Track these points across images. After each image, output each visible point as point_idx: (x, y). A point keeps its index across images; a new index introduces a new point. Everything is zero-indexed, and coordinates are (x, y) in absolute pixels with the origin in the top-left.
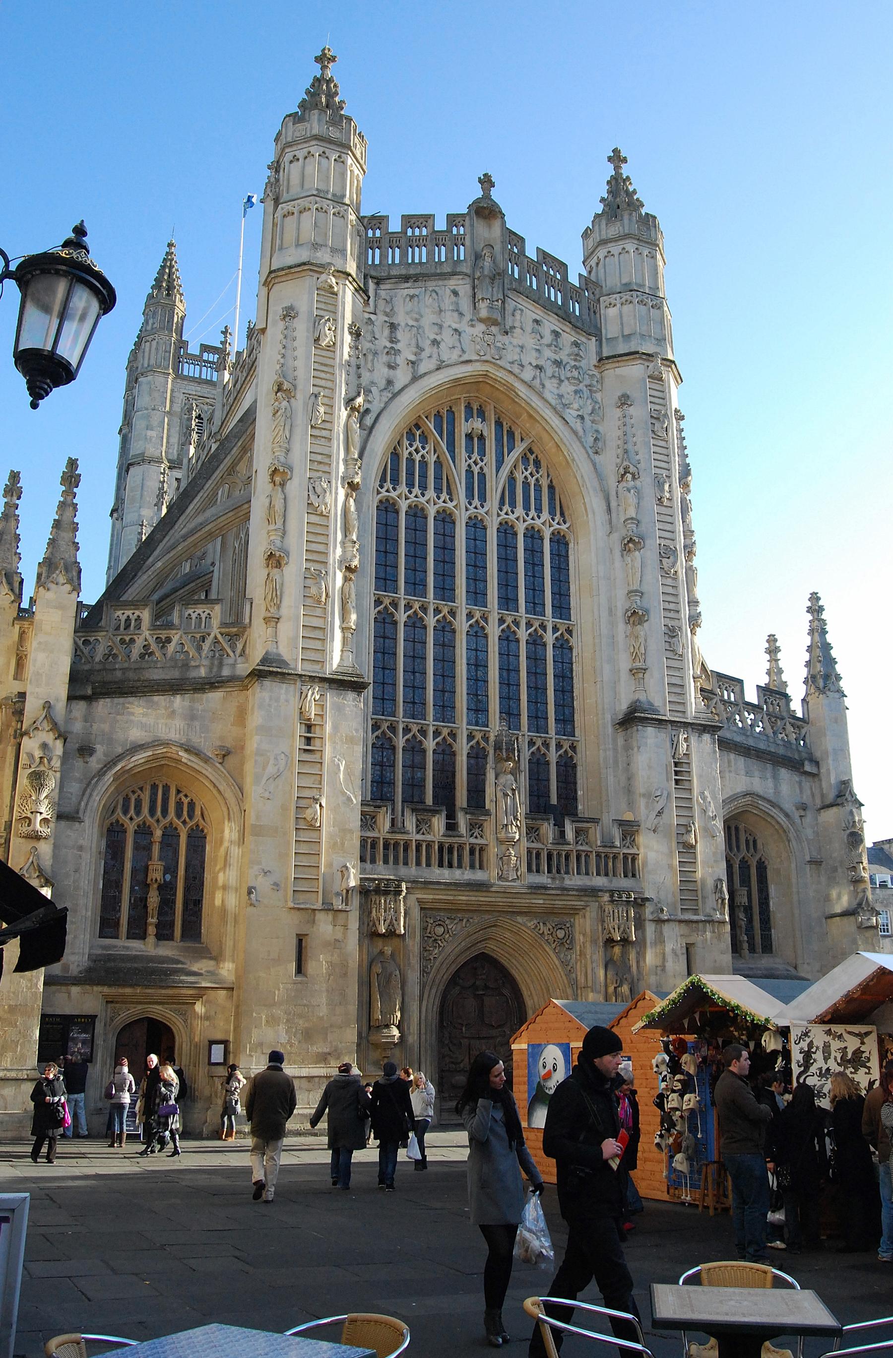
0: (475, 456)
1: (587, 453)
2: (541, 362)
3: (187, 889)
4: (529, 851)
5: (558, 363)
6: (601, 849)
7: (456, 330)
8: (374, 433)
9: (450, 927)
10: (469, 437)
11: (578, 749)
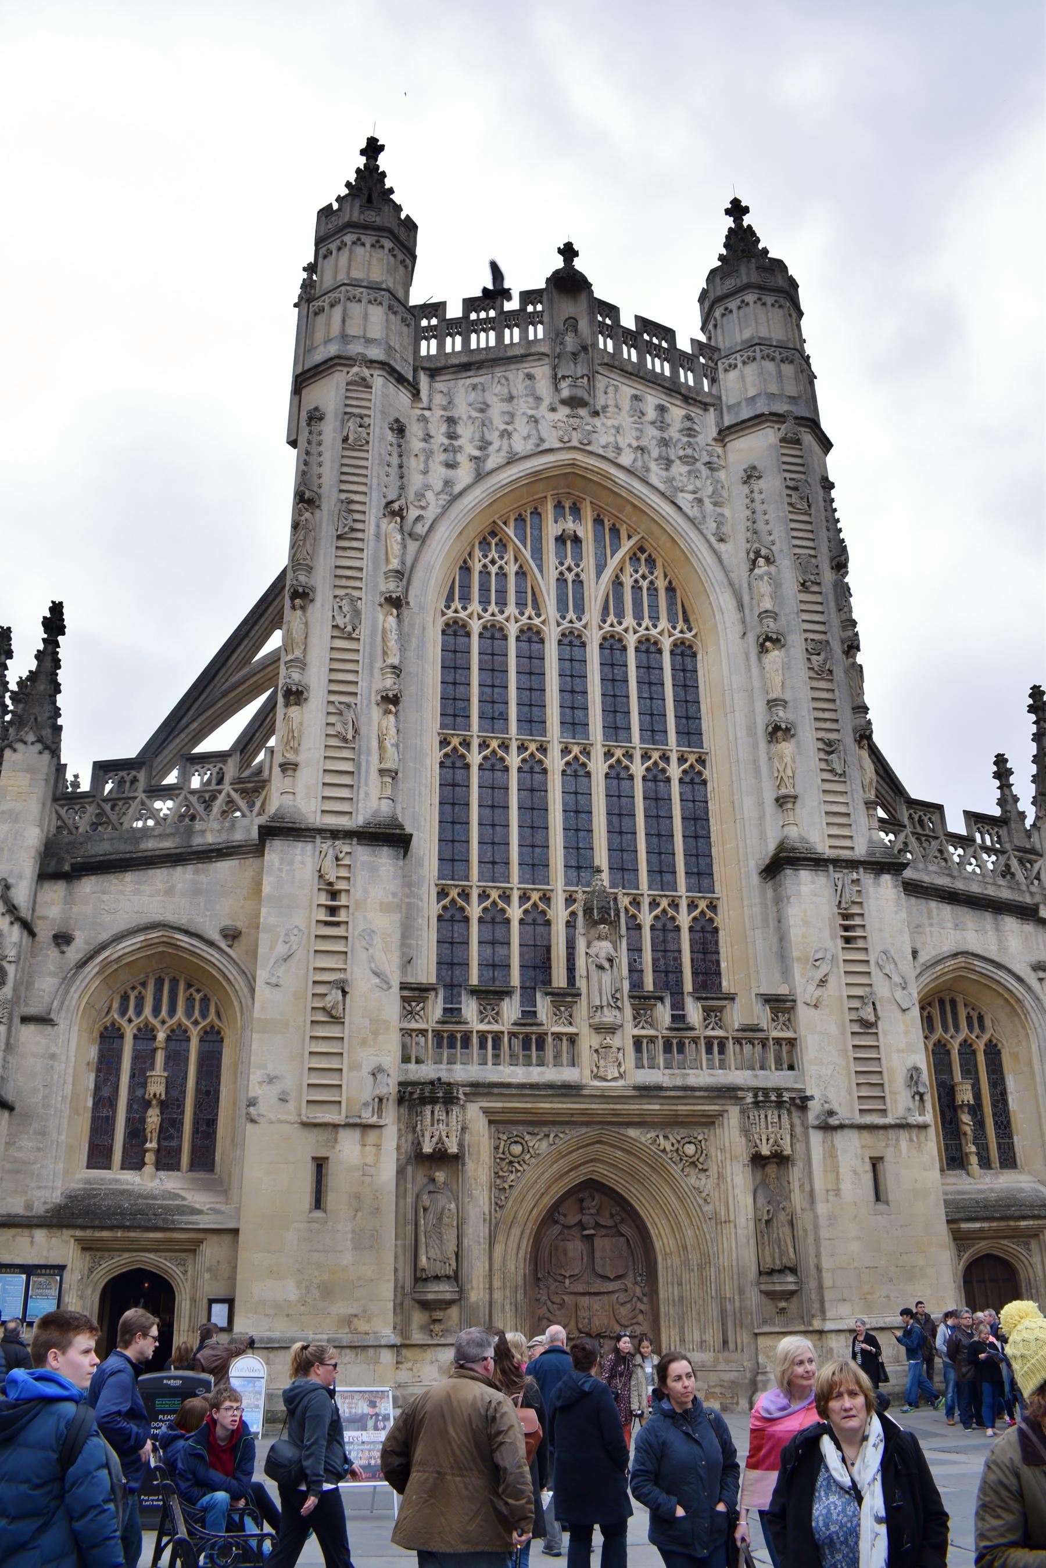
0: (569, 561)
1: (708, 541)
2: (643, 443)
3: (198, 1106)
5: (664, 443)
6: (740, 1035)
7: (532, 416)
8: (428, 542)
9: (531, 1144)
10: (561, 540)
11: (719, 910)
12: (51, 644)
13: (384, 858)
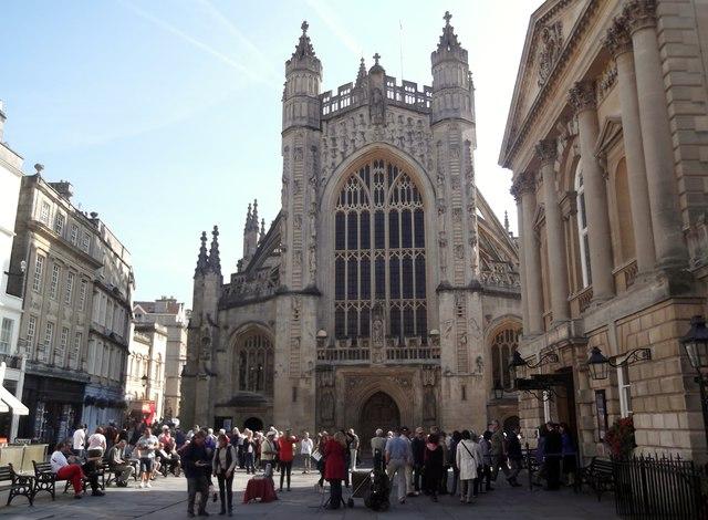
4: (388, 352)
5: (410, 134)
12: (215, 239)
13: (311, 300)
